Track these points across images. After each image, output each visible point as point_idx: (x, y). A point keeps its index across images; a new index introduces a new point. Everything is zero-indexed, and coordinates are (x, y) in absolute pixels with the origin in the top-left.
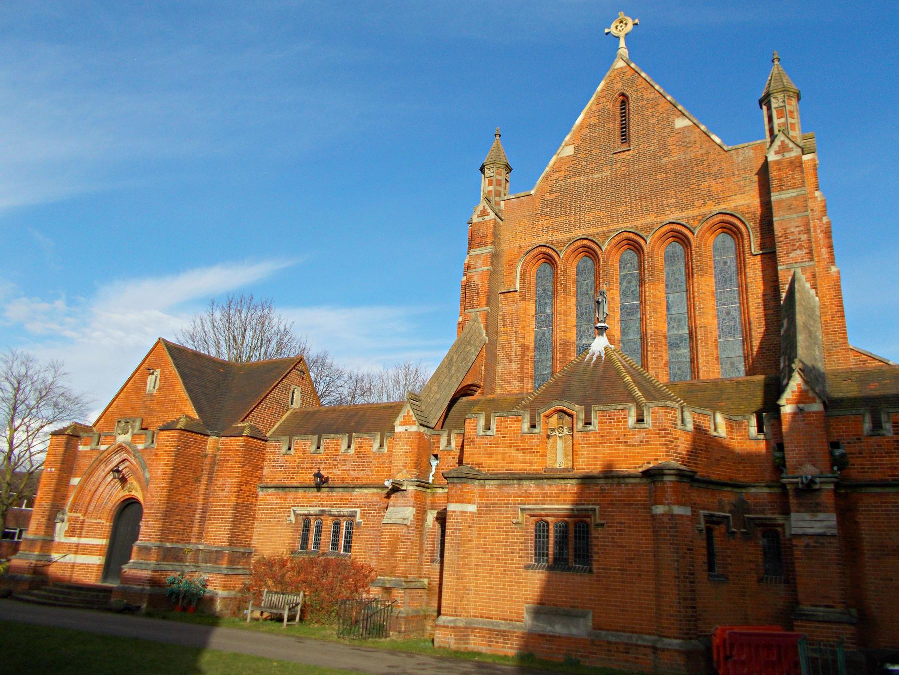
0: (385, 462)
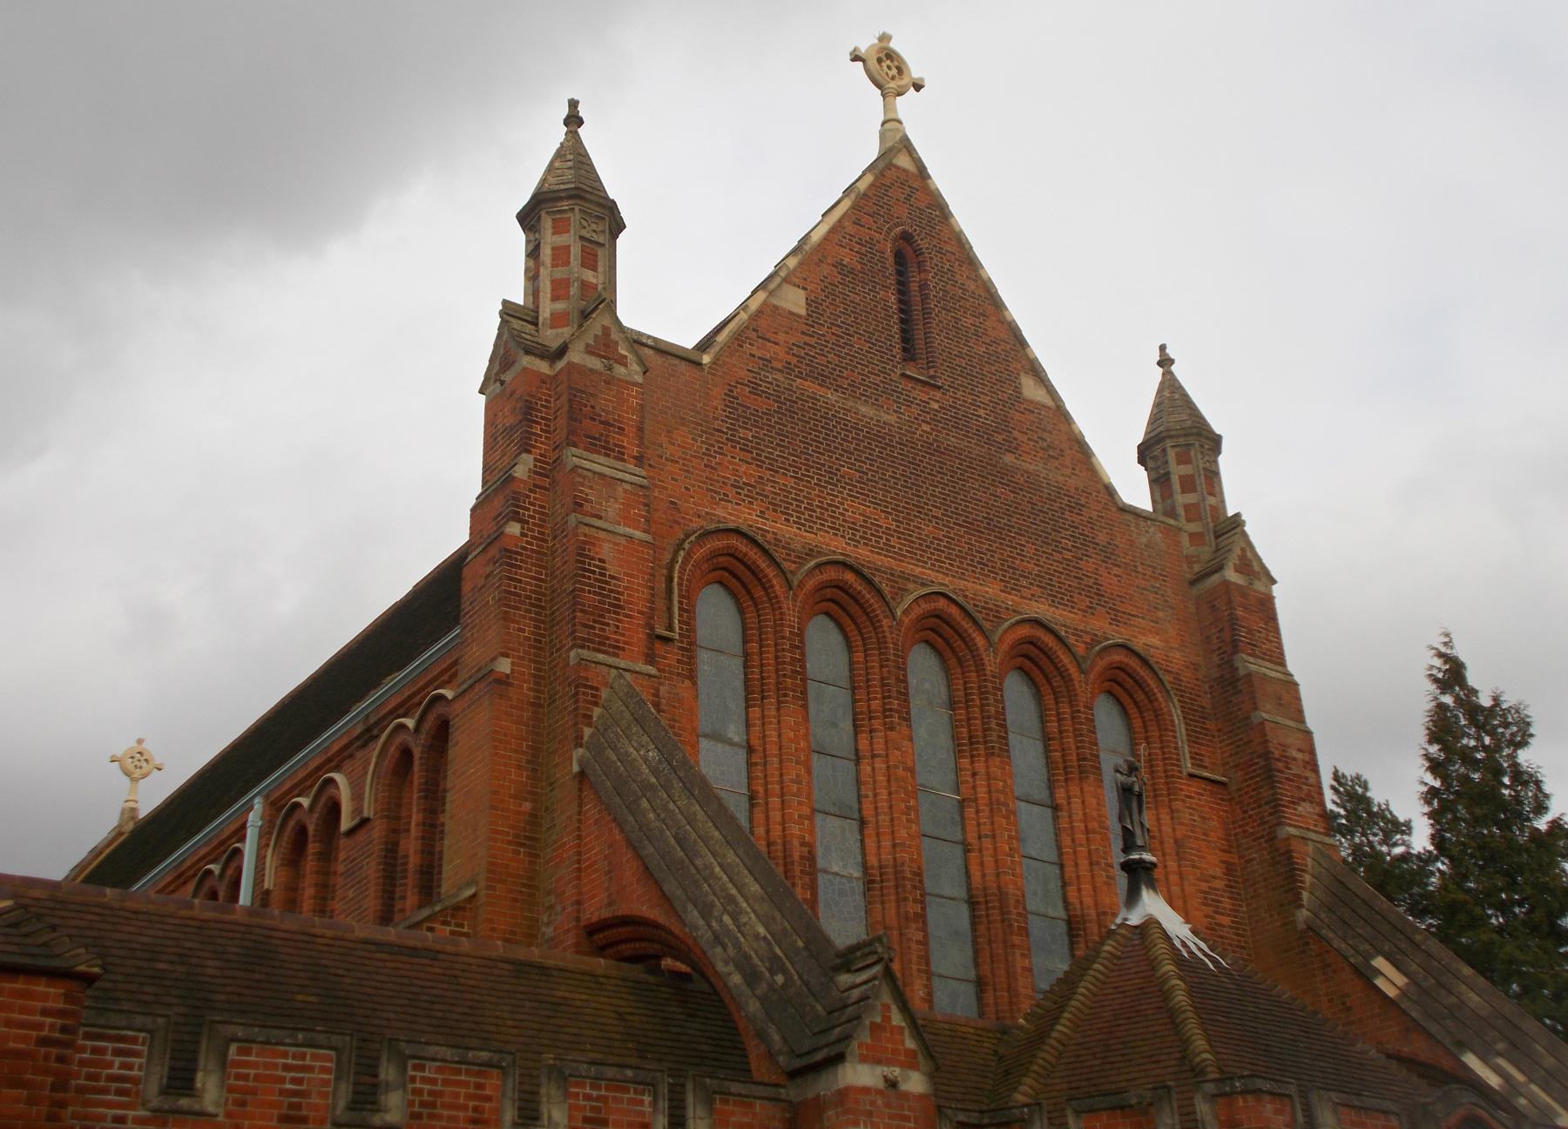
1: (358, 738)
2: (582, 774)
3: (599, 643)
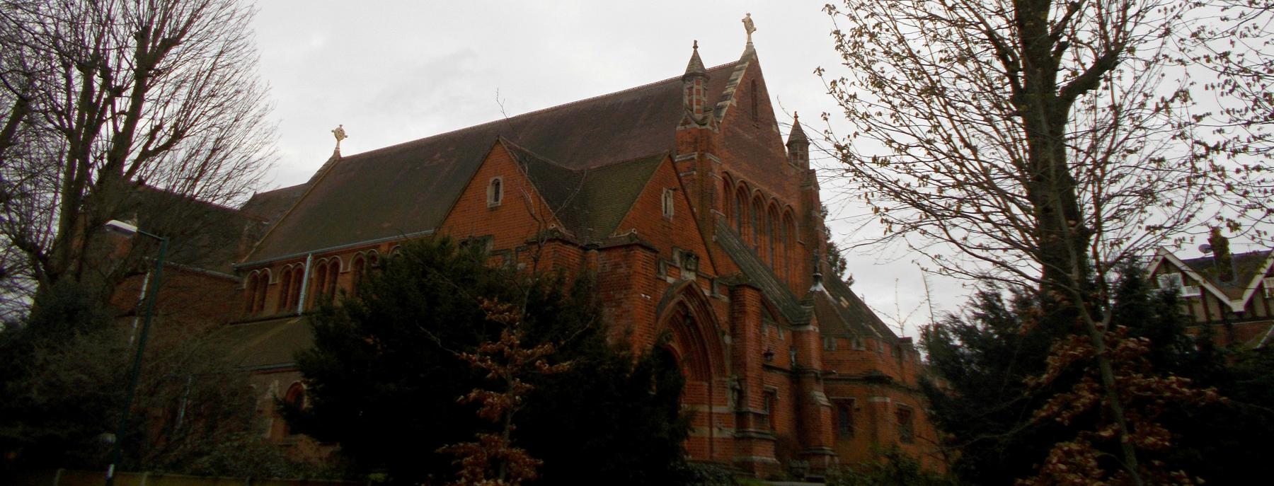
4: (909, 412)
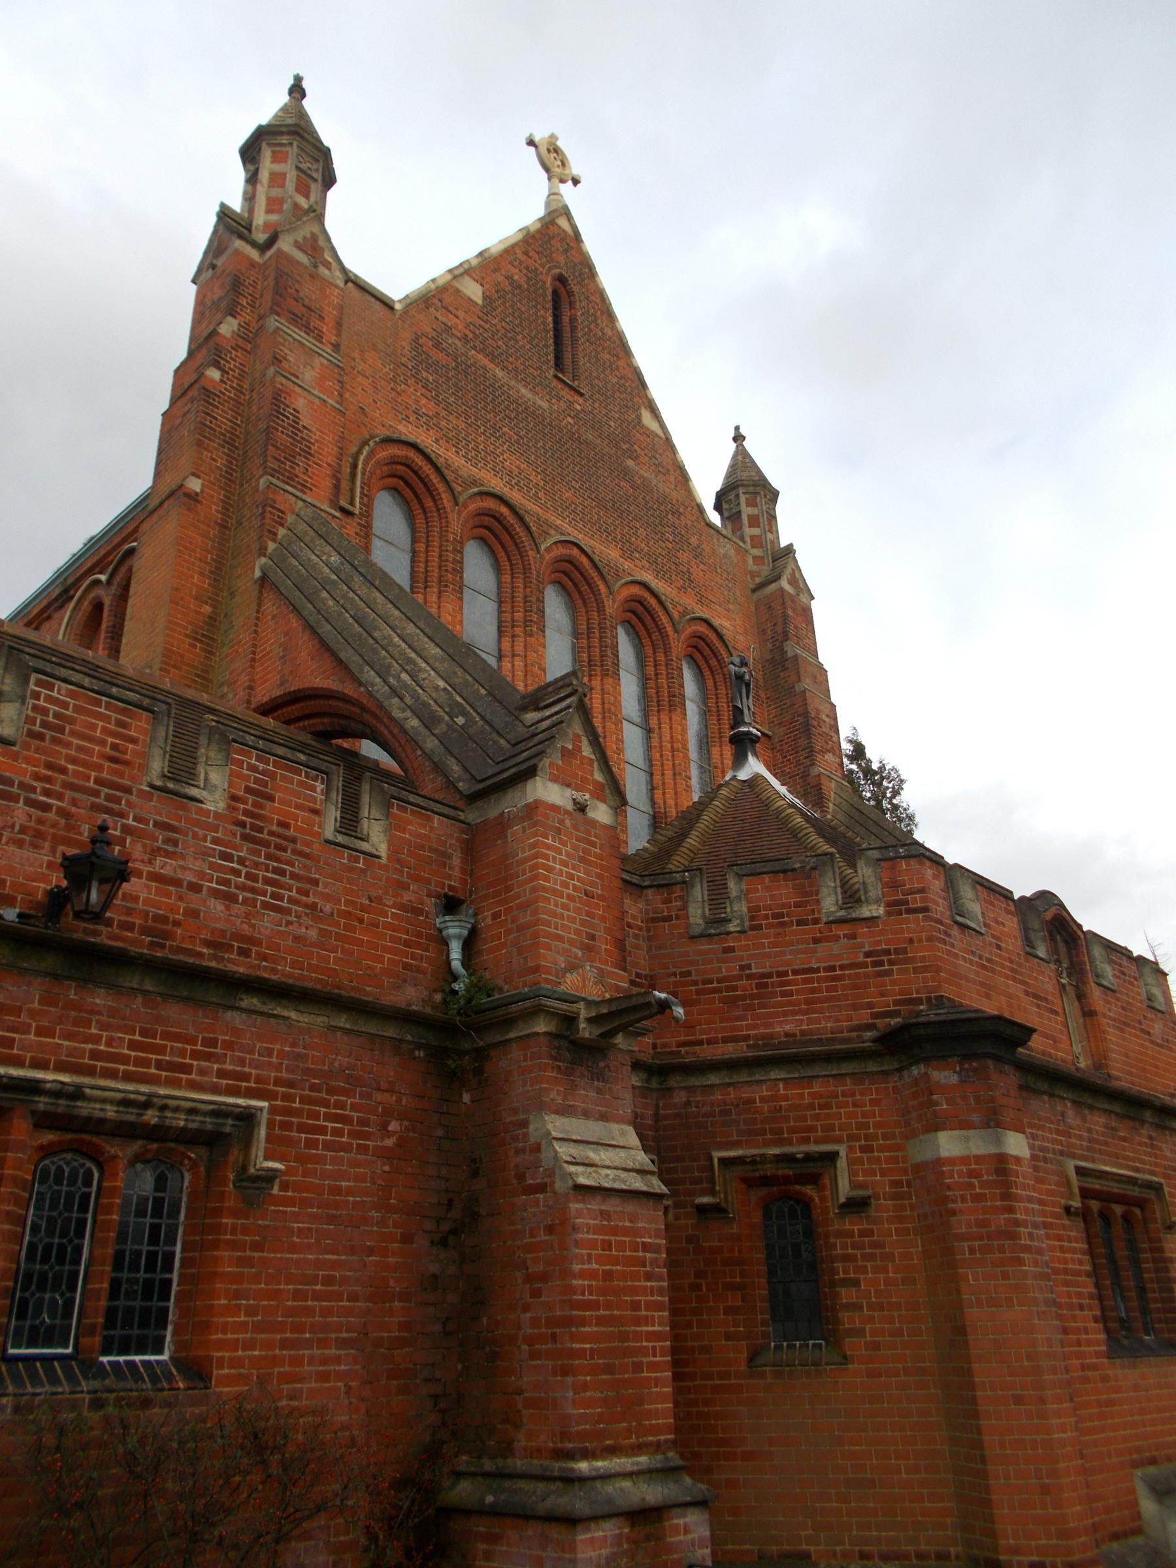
0: (379, 900)
1: (56, 599)
2: (264, 579)
3: (288, 478)
4: (1141, 1203)
